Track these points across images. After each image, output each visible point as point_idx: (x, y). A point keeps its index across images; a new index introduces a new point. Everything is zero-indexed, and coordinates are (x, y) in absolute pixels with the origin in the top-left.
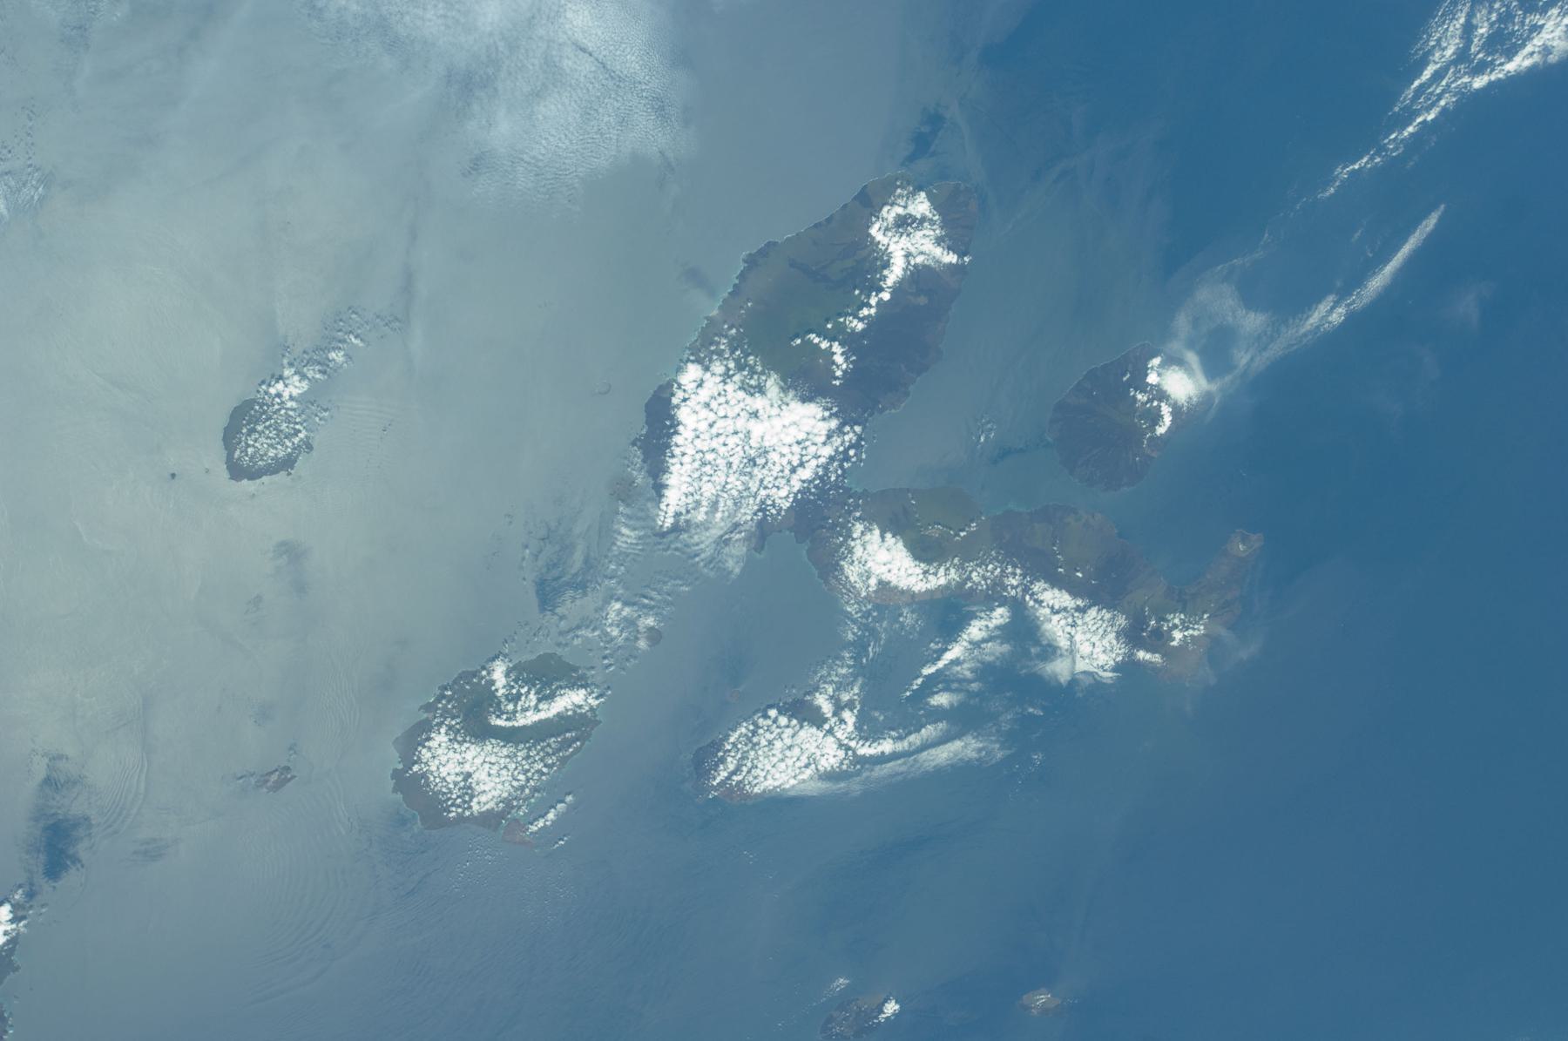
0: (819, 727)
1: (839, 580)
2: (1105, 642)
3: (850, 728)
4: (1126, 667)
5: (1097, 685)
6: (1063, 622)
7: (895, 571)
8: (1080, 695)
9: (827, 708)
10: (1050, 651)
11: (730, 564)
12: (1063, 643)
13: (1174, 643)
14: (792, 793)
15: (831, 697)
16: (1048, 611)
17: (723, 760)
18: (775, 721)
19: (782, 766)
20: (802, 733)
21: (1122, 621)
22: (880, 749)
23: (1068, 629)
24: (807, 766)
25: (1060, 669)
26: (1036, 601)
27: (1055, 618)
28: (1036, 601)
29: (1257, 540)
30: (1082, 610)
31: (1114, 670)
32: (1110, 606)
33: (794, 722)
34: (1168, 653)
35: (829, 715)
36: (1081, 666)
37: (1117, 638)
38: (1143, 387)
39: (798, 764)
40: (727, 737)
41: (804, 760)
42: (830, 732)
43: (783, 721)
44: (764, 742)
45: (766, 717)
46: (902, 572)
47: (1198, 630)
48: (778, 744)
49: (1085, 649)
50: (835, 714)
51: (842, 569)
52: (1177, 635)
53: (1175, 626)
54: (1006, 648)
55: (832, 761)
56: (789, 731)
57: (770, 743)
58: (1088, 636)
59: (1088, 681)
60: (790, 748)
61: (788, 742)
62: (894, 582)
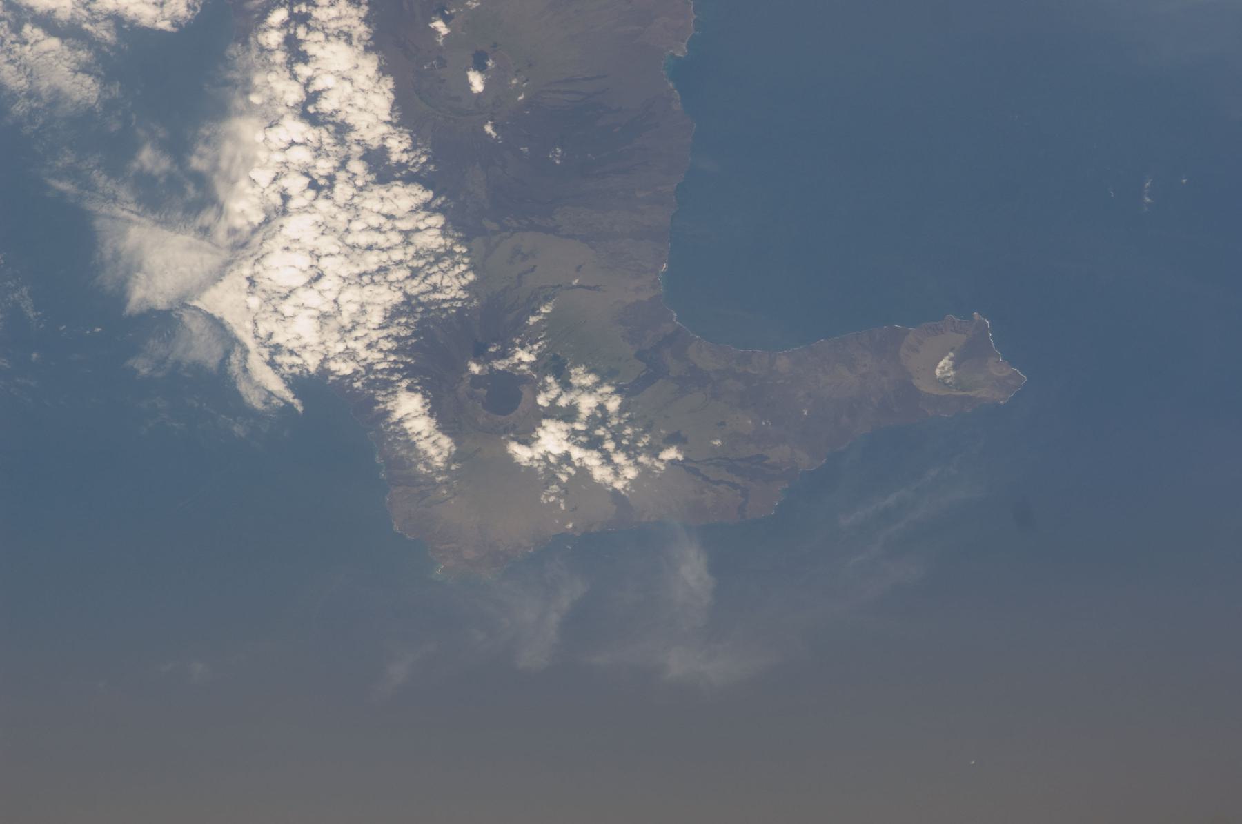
2: (352, 298)
4: (334, 410)
5: (216, 384)
6: (301, 155)
8: (142, 366)
10: (187, 196)
12: (244, 207)
13: (521, 453)
16: (294, 94)
21: (452, 284)
23: (295, 184)
25: (161, 261)
27: (294, 129)
29: (998, 379)
30: (382, 169)
31: (299, 383)
32: (461, 221)
34: (479, 461)
36: (227, 301)
37: (393, 314)
47: (614, 473)
49: (282, 267)
52: (552, 439)
53: (569, 414)
54: (84, 89)
58: (328, 244)
59: (204, 351)
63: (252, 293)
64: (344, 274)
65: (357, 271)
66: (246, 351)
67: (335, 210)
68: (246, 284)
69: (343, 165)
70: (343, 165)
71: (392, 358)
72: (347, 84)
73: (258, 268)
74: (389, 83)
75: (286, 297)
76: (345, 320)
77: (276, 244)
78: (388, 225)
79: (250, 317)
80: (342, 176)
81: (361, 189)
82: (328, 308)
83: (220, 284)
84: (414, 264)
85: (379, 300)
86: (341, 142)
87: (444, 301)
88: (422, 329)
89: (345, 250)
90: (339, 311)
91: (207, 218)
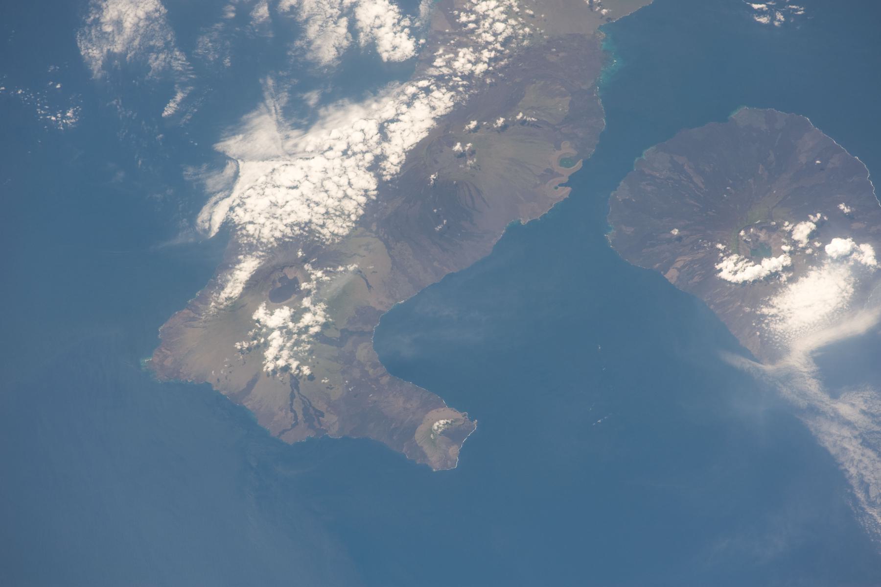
12: (313, 139)
26: (414, 97)
28: (414, 97)
38: (821, 234)
63: (267, 176)
64: (305, 193)
65: (311, 196)
66: (228, 196)
67: (338, 166)
68: (270, 170)
69: (364, 153)
70: (364, 153)
71: (272, 240)
72: (411, 124)
73: (283, 168)
74: (425, 134)
75: (274, 186)
76: (279, 211)
77: (300, 163)
78: (344, 188)
79: (252, 184)
80: (359, 156)
81: (358, 166)
82: (281, 202)
83: (261, 162)
84: (332, 211)
85: (300, 214)
86: (379, 143)
87: (320, 233)
88: (296, 239)
89: (319, 185)
90: (282, 207)
91: (295, 133)
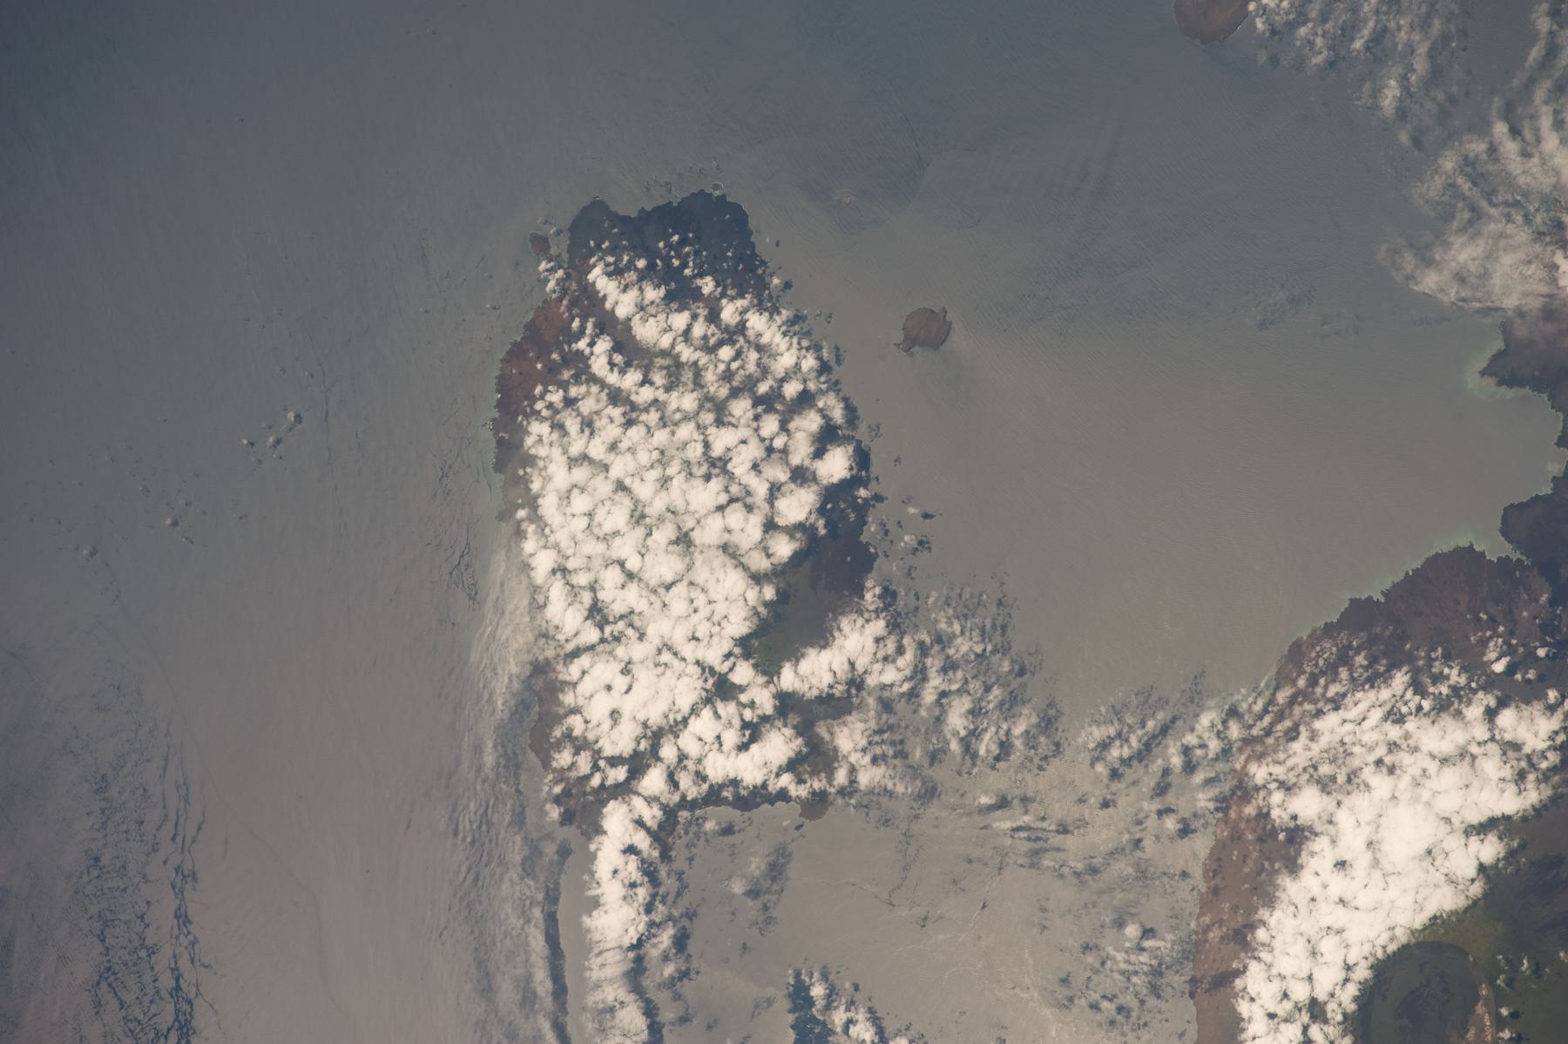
0: (745, 646)
1: (1331, 672)
3: (719, 767)
7: (1338, 885)
9: (814, 671)
11: (1464, 253)
14: (499, 565)
15: (856, 683)
17: (681, 295)
18: (801, 476)
19: (616, 517)
20: (732, 582)
22: (611, 892)
24: (597, 613)
33: (784, 548)
35: (788, 679)
39: (612, 576)
40: (767, 306)
41: (618, 598)
42: (721, 689)
43: (797, 506)
44: (722, 440)
45: (826, 439)
46: (1330, 915)
48: (706, 495)
50: (787, 704)
51: (1374, 680)
55: (598, 709)
56: (747, 529)
57: (718, 466)
60: (684, 540)
61: (709, 533)
62: (1292, 889)
